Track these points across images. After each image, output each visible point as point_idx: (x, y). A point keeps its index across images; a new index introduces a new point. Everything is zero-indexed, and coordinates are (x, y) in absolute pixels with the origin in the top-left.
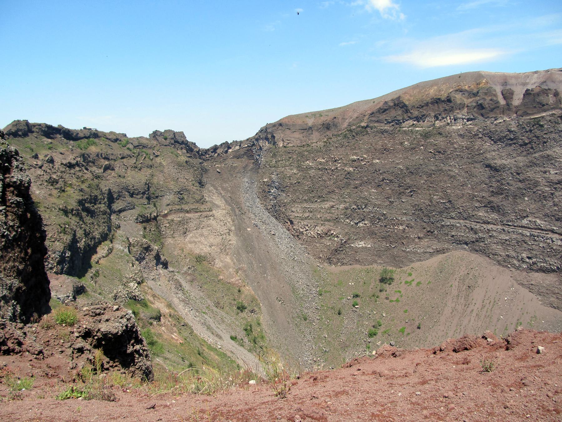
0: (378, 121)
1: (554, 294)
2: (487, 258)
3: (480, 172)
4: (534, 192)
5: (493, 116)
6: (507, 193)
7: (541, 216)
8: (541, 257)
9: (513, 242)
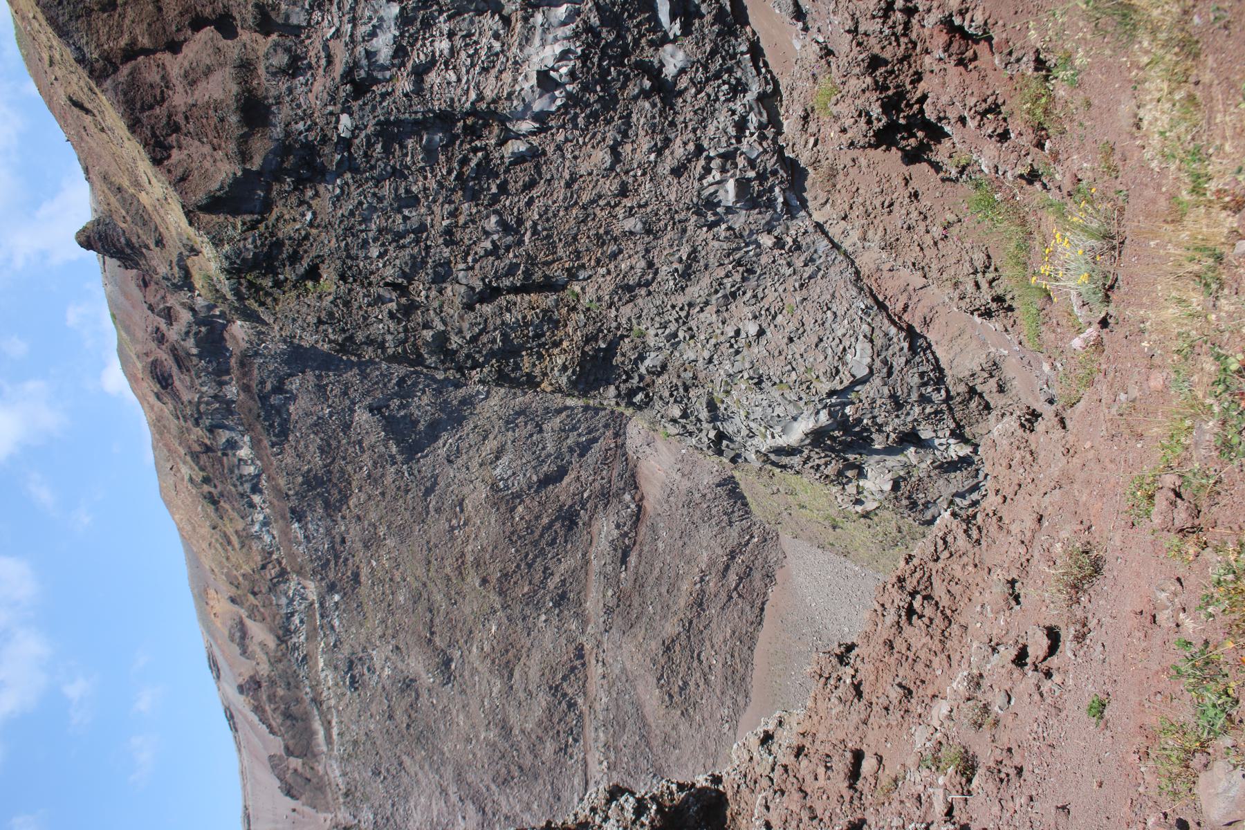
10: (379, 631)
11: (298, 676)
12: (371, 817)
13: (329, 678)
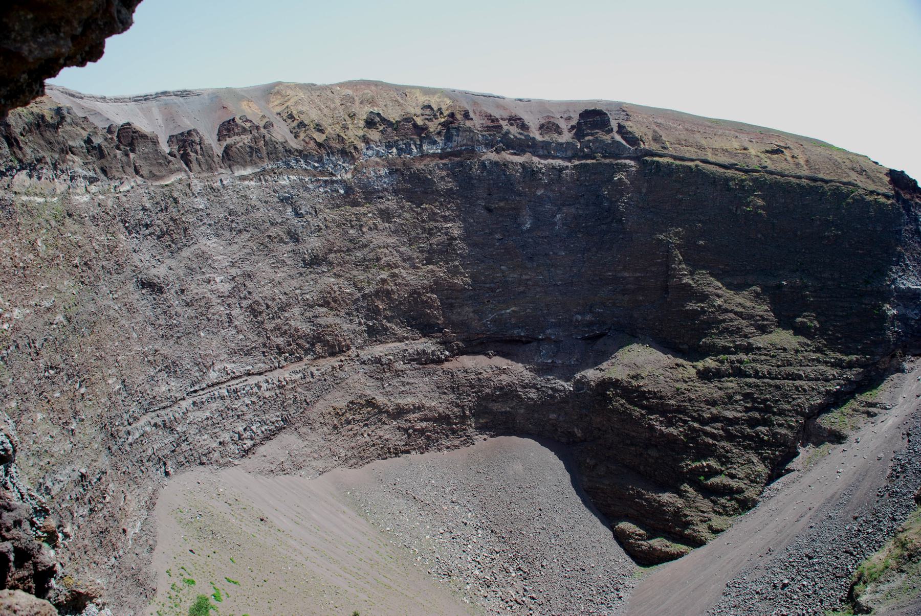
1: (309, 457)
2: (201, 467)
3: (138, 300)
4: (209, 320)
5: (120, 176)
6: (178, 332)
7: (226, 356)
8: (257, 418)
9: (215, 416)
10: (327, 217)
11: (278, 161)
12: (201, 207)
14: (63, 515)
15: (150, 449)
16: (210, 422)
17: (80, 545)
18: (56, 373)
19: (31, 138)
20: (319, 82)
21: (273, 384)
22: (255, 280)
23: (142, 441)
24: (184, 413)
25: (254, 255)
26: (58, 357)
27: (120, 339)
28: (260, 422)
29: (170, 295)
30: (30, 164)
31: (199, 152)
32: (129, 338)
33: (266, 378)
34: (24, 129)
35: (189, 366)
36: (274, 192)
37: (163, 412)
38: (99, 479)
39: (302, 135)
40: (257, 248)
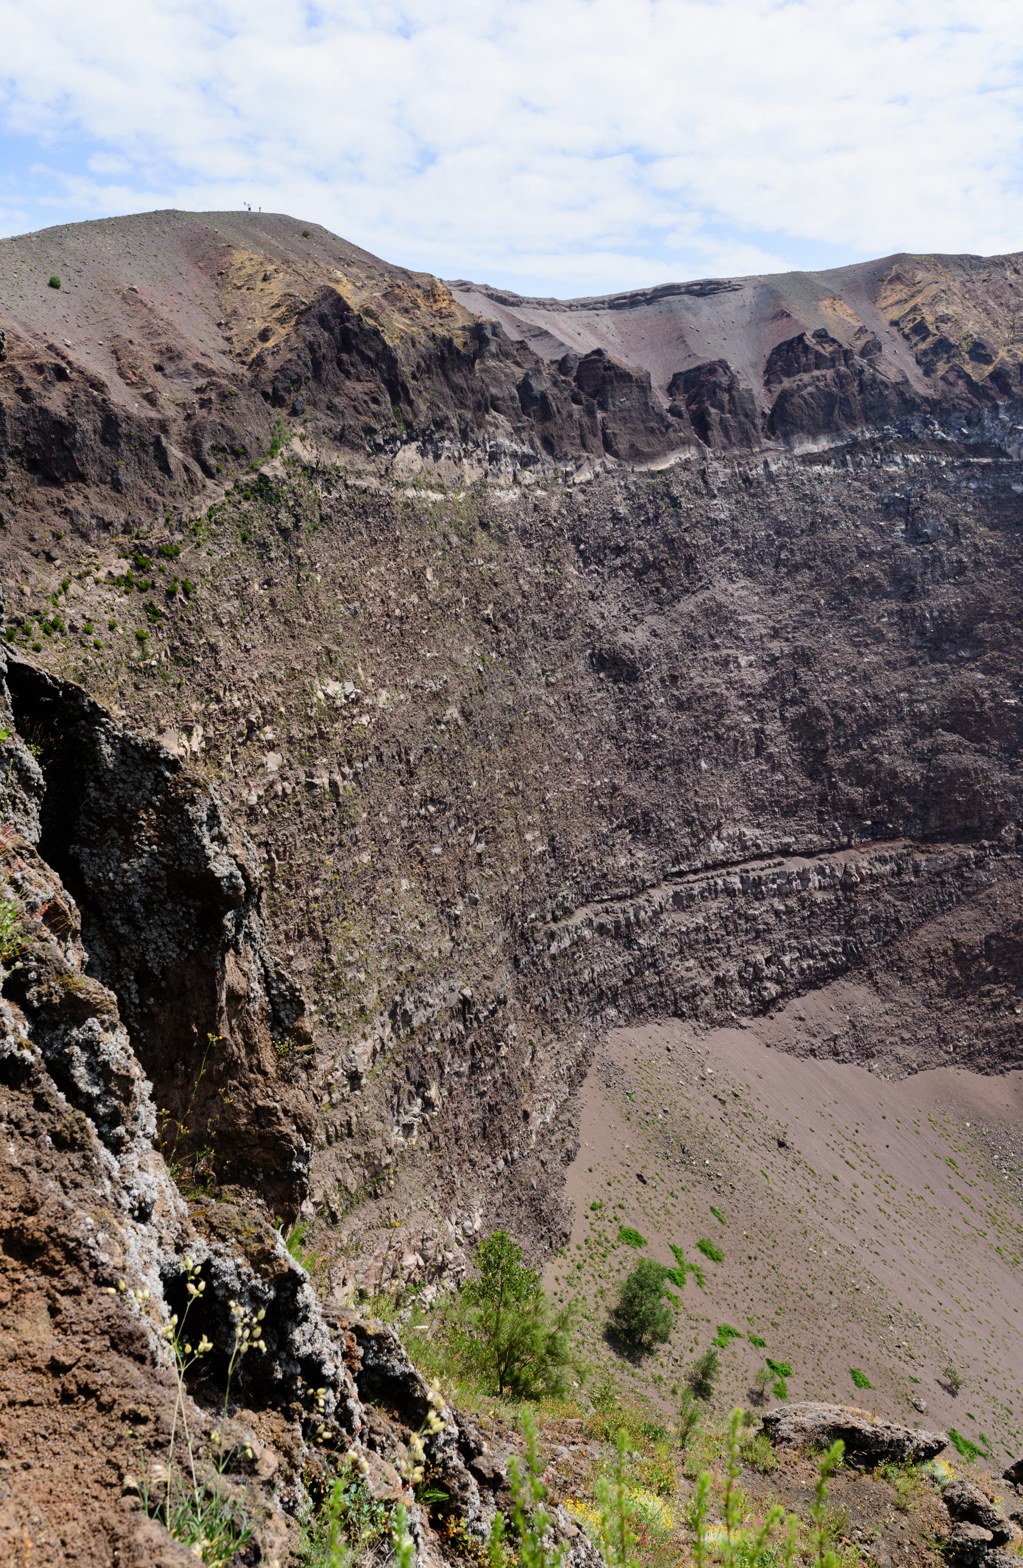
0: (341, 439)
1: (893, 1035)
2: (676, 1019)
4: (718, 738)
5: (576, 454)
6: (660, 756)
7: (746, 812)
8: (794, 943)
9: (714, 927)
10: (981, 544)
11: (886, 423)
12: (722, 516)
13: (895, 468)
14: (426, 1067)
15: (586, 971)
16: (702, 937)
17: (449, 1125)
18: (438, 811)
19: (428, 383)
20: (987, 250)
21: (833, 876)
22: (817, 667)
23: (574, 953)
24: (655, 912)
25: (820, 616)
26: (445, 783)
27: (554, 760)
28: (799, 951)
29: (651, 685)
30: (424, 431)
31: (727, 406)
32: (568, 760)
33: (822, 863)
34: (419, 366)
35: (673, 824)
36: (871, 489)
37: (617, 906)
38: (493, 1012)
39: (942, 368)
40: (827, 603)
